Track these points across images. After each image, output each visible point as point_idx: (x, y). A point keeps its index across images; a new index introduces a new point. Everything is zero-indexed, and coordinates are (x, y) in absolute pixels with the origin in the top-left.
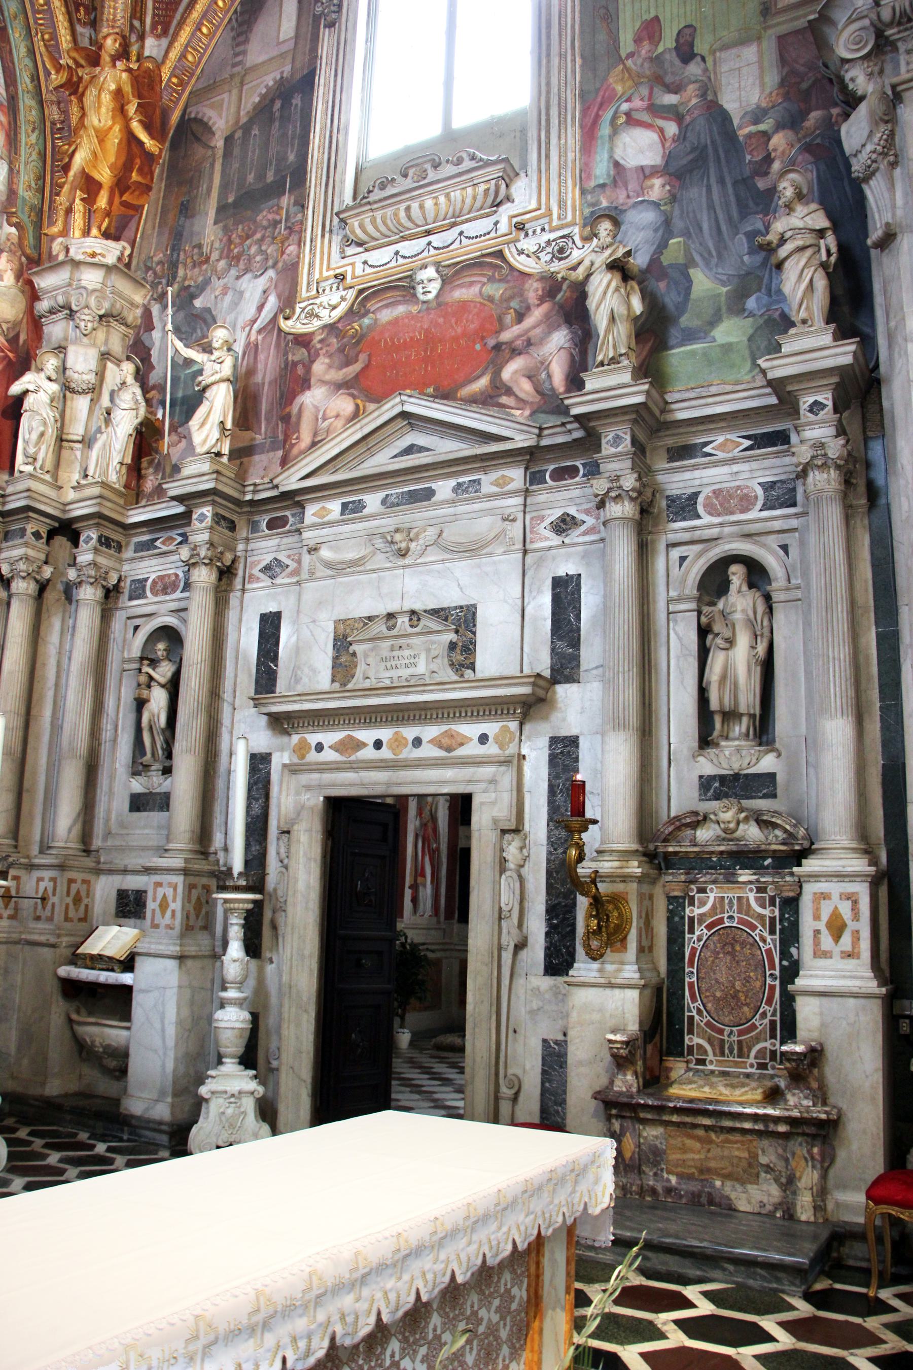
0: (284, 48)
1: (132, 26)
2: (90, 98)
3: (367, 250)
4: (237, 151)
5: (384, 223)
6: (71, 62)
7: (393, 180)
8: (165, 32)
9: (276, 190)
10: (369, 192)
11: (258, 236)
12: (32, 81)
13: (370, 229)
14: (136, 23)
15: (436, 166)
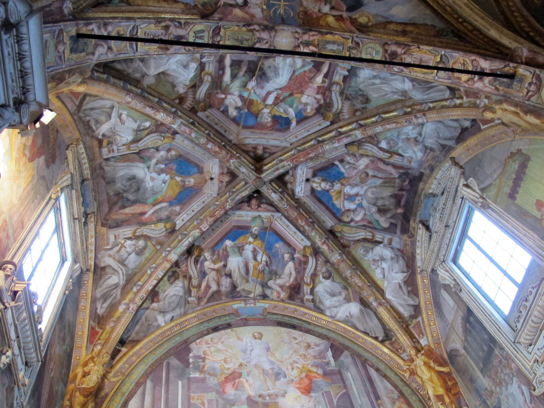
0: (455, 308)
1: (414, 342)
2: (419, 372)
3: (535, 345)
4: (470, 349)
5: (530, 332)
6: (407, 367)
7: (519, 316)
8: (423, 335)
9: (491, 351)
10: (516, 327)
11: (499, 370)
12: (401, 381)
13: (528, 337)
14: (414, 340)
15: (526, 301)
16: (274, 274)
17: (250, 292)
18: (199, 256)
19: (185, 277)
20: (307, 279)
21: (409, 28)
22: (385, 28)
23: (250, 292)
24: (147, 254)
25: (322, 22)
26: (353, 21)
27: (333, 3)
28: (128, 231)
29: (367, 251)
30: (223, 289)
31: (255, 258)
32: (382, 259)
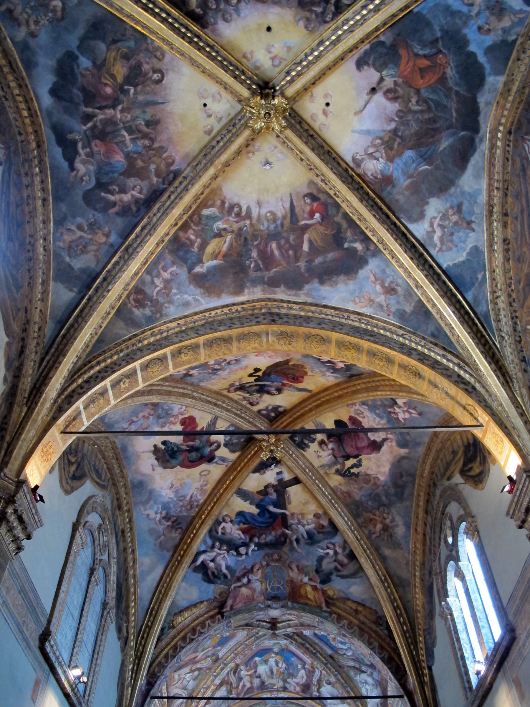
16: (291, 675)
17: (275, 685)
18: (236, 669)
19: (227, 683)
20: (315, 682)
21: (360, 608)
22: (344, 603)
23: (275, 685)
24: (200, 677)
25: (302, 592)
26: (324, 592)
28: (187, 669)
29: (356, 675)
30: (255, 685)
31: (277, 665)
32: (366, 683)
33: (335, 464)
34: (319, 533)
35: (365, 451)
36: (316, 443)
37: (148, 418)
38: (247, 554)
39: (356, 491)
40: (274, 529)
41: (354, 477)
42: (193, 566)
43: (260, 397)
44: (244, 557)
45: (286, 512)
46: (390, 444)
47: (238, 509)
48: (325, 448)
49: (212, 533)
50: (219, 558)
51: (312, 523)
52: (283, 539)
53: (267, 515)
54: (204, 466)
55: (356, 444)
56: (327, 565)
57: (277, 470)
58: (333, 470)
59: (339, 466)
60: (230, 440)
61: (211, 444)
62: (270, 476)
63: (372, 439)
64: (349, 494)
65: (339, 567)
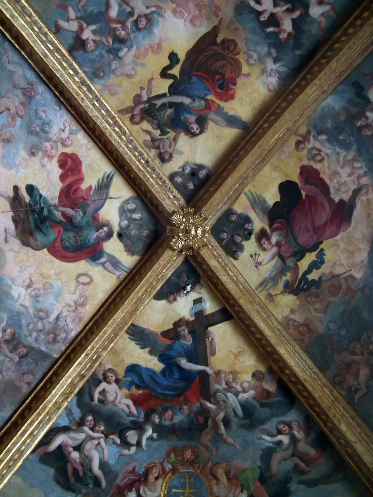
27: (252, 489)
33: (282, 272)
34: (262, 405)
35: (328, 232)
36: (253, 237)
37: (13, 118)
38: (139, 444)
39: (319, 315)
40: (187, 401)
41: (313, 289)
42: (41, 451)
43: (175, 139)
44: (133, 449)
45: (208, 369)
46: (364, 198)
47: (129, 361)
48: (266, 245)
49: (83, 397)
50: (89, 446)
51: (250, 388)
52: (201, 420)
53: (177, 375)
54: (82, 266)
55: (313, 224)
56: (280, 465)
57: (194, 295)
58: (281, 286)
59: (288, 277)
60: (128, 226)
61: (100, 226)
62: (183, 306)
63: (337, 200)
64: (306, 325)
65: (302, 464)
